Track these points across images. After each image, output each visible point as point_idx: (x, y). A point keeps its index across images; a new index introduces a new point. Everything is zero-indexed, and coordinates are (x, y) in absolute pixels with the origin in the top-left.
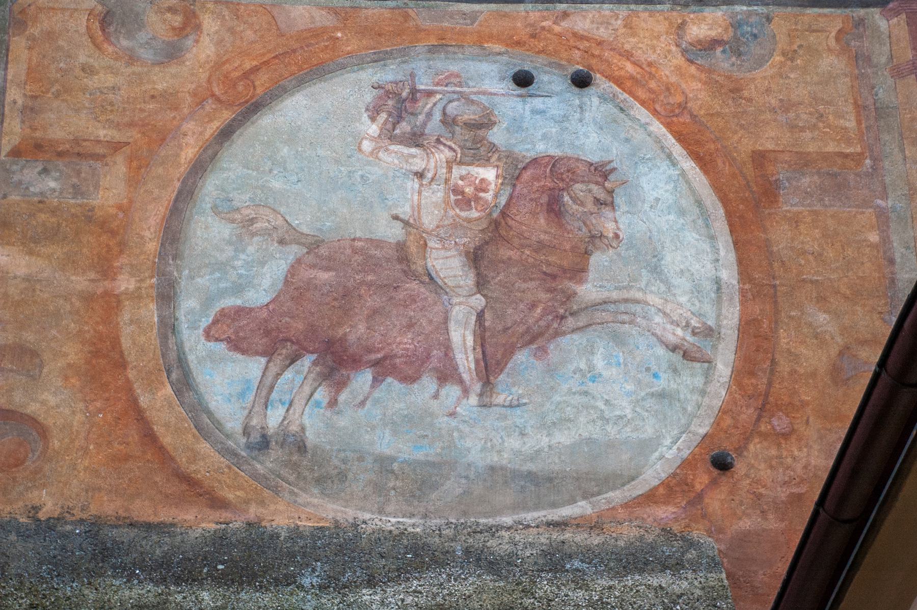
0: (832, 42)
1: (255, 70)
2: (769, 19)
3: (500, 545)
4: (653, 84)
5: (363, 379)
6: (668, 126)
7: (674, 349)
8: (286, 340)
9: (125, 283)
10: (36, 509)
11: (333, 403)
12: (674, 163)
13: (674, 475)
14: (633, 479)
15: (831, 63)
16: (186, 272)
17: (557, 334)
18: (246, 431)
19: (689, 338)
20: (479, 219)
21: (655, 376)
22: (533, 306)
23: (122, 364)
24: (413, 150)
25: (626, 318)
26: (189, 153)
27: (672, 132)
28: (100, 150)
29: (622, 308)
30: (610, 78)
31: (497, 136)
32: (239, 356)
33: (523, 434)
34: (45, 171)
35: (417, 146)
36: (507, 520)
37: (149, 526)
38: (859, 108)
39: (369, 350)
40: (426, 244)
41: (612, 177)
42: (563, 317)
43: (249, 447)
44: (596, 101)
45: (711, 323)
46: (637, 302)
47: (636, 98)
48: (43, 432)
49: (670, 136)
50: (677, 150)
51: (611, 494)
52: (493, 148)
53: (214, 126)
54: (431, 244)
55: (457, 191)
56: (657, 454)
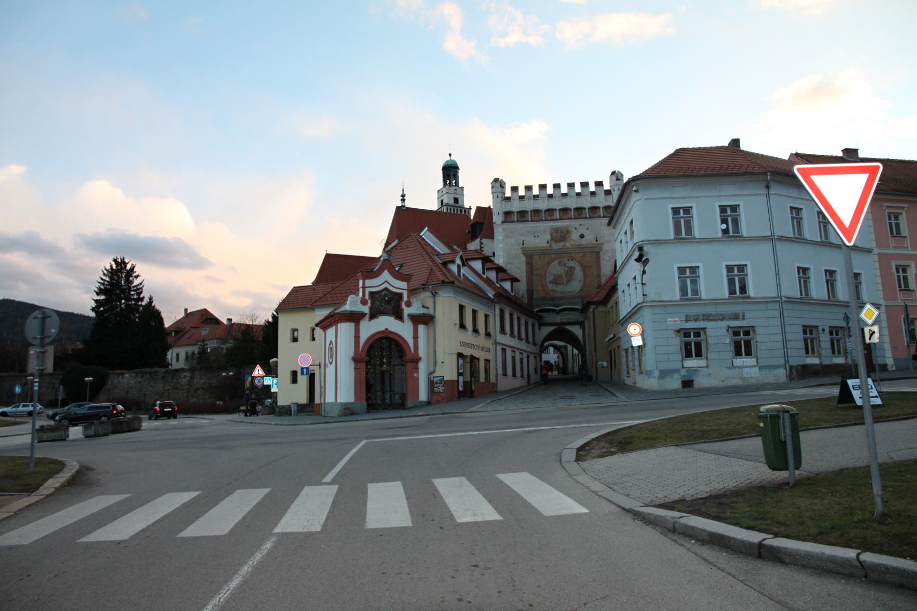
5: (558, 286)
31: (567, 265)
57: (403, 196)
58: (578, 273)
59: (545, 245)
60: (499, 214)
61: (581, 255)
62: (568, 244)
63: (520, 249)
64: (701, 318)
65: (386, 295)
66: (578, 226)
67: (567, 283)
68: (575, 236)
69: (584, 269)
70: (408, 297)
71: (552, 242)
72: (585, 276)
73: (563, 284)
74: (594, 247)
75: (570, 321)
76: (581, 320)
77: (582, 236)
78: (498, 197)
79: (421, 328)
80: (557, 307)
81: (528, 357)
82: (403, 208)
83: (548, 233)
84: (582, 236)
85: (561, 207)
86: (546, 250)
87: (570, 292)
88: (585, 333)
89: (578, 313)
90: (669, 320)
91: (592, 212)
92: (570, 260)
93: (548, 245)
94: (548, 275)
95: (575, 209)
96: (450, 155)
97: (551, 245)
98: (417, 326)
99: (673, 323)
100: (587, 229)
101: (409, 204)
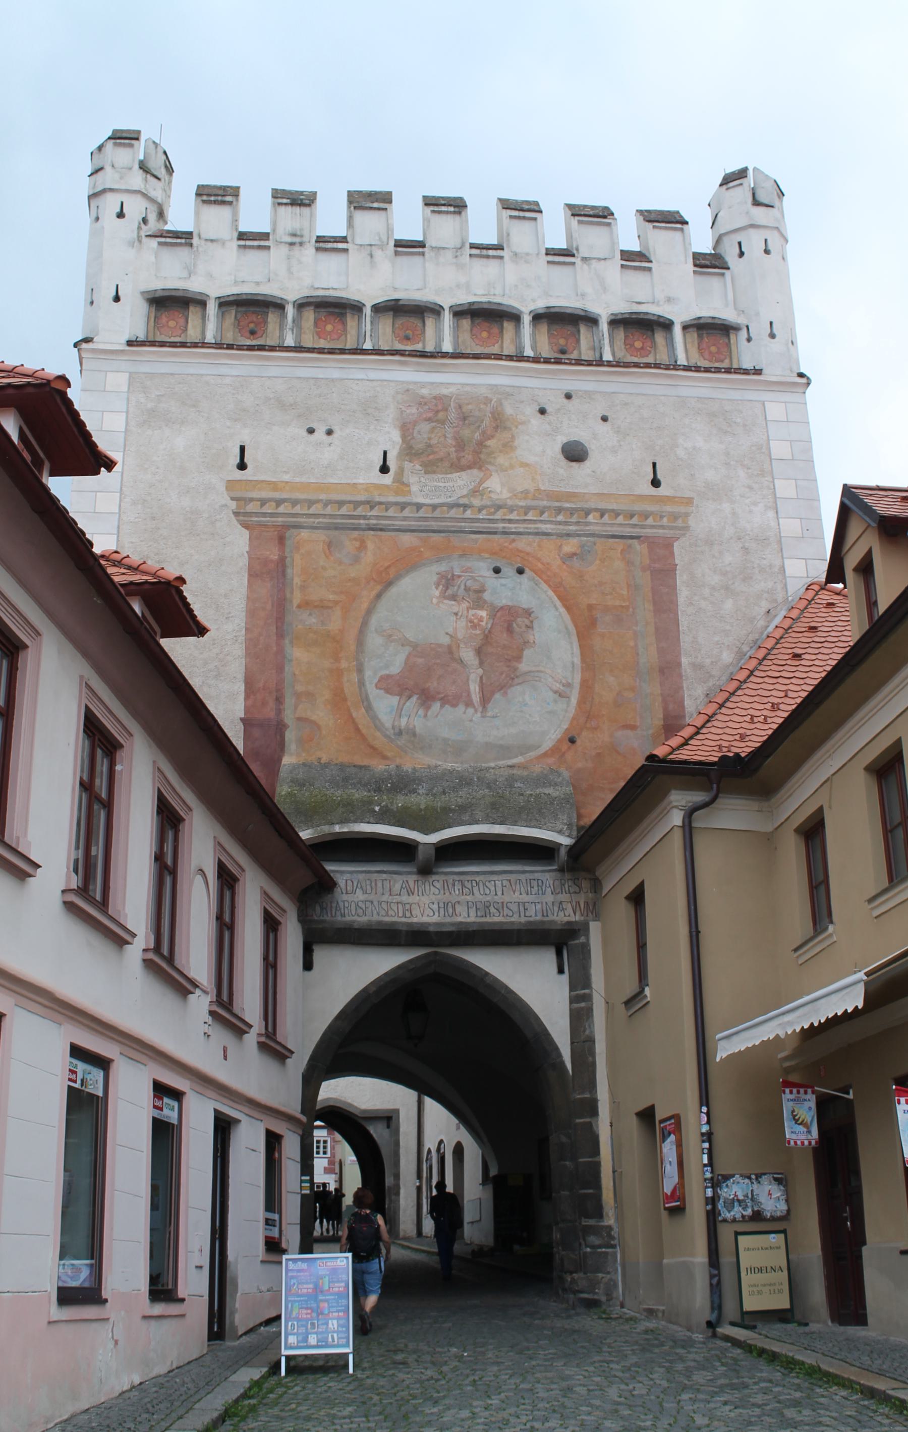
0: (619, 555)
1: (389, 567)
2: (595, 544)
3: (489, 776)
4: (549, 573)
5: (436, 706)
6: (554, 592)
7: (555, 692)
8: (407, 689)
9: (344, 664)
10: (320, 759)
11: (425, 716)
12: (557, 609)
13: (554, 746)
14: (539, 747)
15: (619, 564)
16: (366, 659)
17: (511, 686)
18: (393, 727)
19: (562, 688)
20: (479, 634)
21: (548, 704)
22: (502, 674)
23: (345, 700)
24: (453, 603)
25: (537, 679)
26: (365, 606)
27: (556, 595)
28: (330, 605)
29: (536, 674)
30: (531, 570)
31: (486, 596)
32: (389, 696)
33: (498, 729)
34: (310, 614)
35: (455, 600)
36: (492, 765)
37: (360, 767)
38: (629, 586)
39: (439, 693)
40: (459, 646)
41: (532, 615)
42: (513, 679)
43: (395, 734)
44: (526, 580)
45: (570, 681)
46: (541, 672)
47: (542, 579)
48: (319, 728)
49: (555, 597)
50: (558, 603)
51: (531, 754)
52: (485, 602)
53: (374, 593)
54: (461, 646)
55: (471, 622)
56: (548, 737)
60: (117, 299)
61: (570, 546)
63: (222, 488)
66: (554, 402)
67: (485, 700)
71: (407, 465)
74: (645, 516)
75: (496, 918)
78: (121, 215)
83: (390, 415)
85: (463, 298)
86: (372, 505)
87: (505, 750)
88: (588, 998)
92: (509, 571)
93: (387, 479)
94: (374, 641)
95: (537, 318)
100: (605, 419)
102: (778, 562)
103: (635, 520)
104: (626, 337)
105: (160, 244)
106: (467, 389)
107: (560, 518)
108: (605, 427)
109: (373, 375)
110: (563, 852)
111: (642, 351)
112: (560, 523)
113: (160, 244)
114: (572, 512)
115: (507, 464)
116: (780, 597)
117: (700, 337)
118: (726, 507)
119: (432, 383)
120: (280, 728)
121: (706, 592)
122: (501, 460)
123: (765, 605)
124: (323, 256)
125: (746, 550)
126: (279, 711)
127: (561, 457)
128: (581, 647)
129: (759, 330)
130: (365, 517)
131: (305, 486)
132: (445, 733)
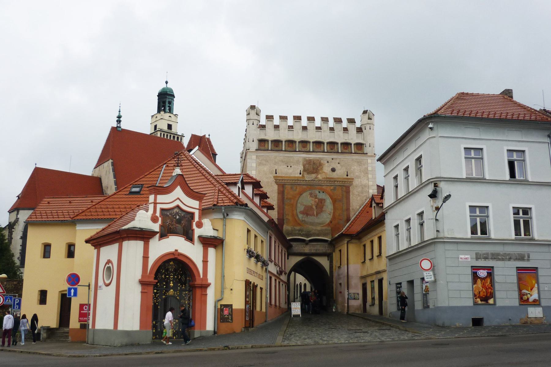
5: (309, 216)
31: (318, 197)
38: (342, 195)
50: (330, 198)
57: (119, 117)
58: (329, 203)
59: (299, 175)
60: (253, 141)
61: (332, 188)
62: (320, 177)
63: (273, 177)
64: (490, 257)
65: (177, 213)
66: (330, 160)
67: (317, 215)
68: (327, 169)
69: (334, 201)
70: (200, 218)
71: (304, 173)
72: (335, 208)
73: (313, 215)
76: (329, 251)
77: (333, 170)
78: (253, 124)
79: (211, 251)
80: (307, 238)
81: (282, 284)
82: (119, 129)
83: (301, 163)
84: (333, 170)
86: (298, 180)
89: (326, 244)
90: (461, 256)
91: (344, 148)
93: (301, 176)
94: (299, 205)
95: (328, 143)
96: (167, 82)
97: (303, 176)
98: (208, 249)
99: (464, 260)
100: (339, 163)
101: (124, 126)
102: (368, 190)
103: (343, 183)
104: (343, 146)
105: (260, 129)
106: (315, 158)
107: (330, 182)
108: (339, 165)
109: (298, 156)
110: (329, 242)
111: (346, 149)
112: (330, 183)
113: (260, 129)
114: (332, 181)
115: (321, 173)
116: (368, 196)
117: (357, 146)
118: (359, 180)
119: (309, 157)
120: (283, 220)
121: (355, 195)
122: (320, 172)
123: (365, 198)
124: (289, 131)
125: (362, 188)
126: (283, 217)
127: (331, 171)
128: (333, 206)
129: (368, 145)
130: (297, 183)
131: (287, 177)
132: (310, 221)
